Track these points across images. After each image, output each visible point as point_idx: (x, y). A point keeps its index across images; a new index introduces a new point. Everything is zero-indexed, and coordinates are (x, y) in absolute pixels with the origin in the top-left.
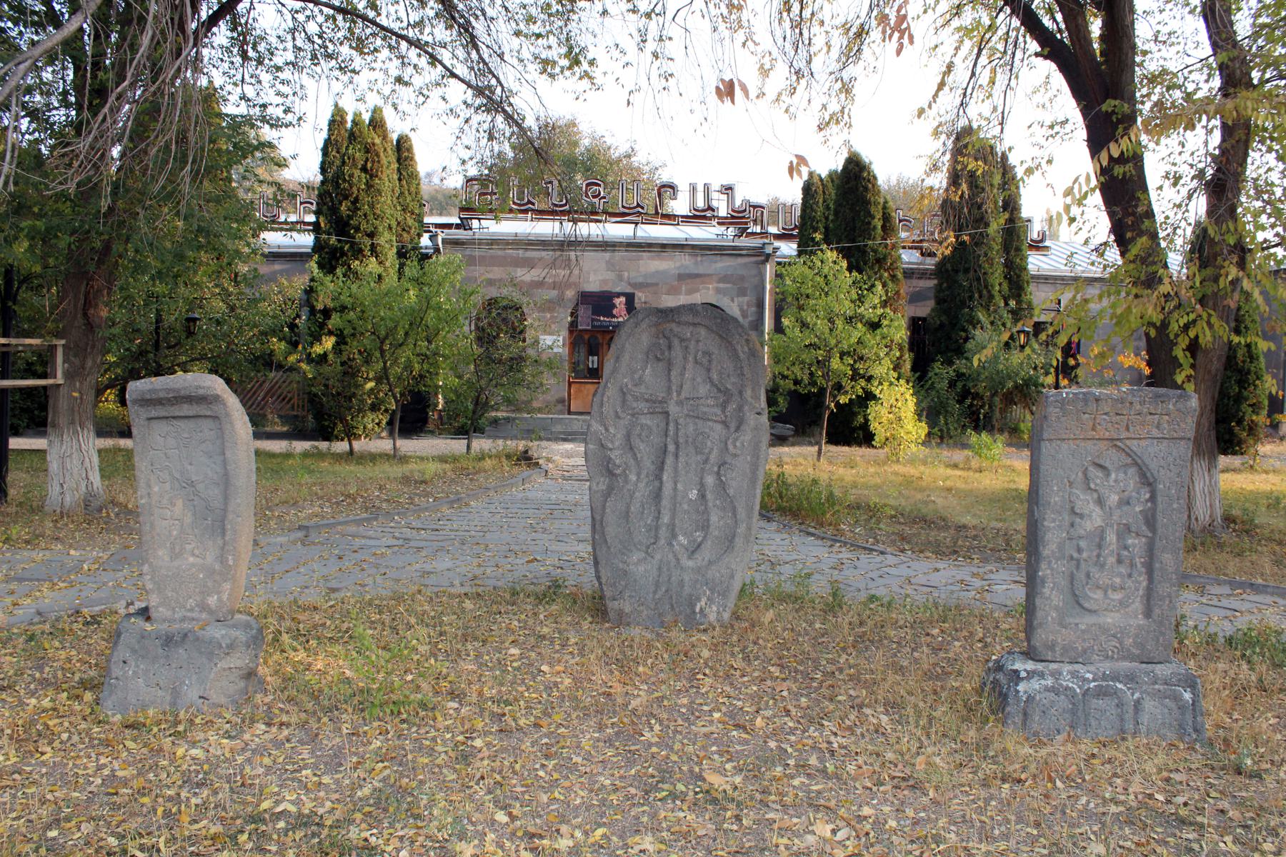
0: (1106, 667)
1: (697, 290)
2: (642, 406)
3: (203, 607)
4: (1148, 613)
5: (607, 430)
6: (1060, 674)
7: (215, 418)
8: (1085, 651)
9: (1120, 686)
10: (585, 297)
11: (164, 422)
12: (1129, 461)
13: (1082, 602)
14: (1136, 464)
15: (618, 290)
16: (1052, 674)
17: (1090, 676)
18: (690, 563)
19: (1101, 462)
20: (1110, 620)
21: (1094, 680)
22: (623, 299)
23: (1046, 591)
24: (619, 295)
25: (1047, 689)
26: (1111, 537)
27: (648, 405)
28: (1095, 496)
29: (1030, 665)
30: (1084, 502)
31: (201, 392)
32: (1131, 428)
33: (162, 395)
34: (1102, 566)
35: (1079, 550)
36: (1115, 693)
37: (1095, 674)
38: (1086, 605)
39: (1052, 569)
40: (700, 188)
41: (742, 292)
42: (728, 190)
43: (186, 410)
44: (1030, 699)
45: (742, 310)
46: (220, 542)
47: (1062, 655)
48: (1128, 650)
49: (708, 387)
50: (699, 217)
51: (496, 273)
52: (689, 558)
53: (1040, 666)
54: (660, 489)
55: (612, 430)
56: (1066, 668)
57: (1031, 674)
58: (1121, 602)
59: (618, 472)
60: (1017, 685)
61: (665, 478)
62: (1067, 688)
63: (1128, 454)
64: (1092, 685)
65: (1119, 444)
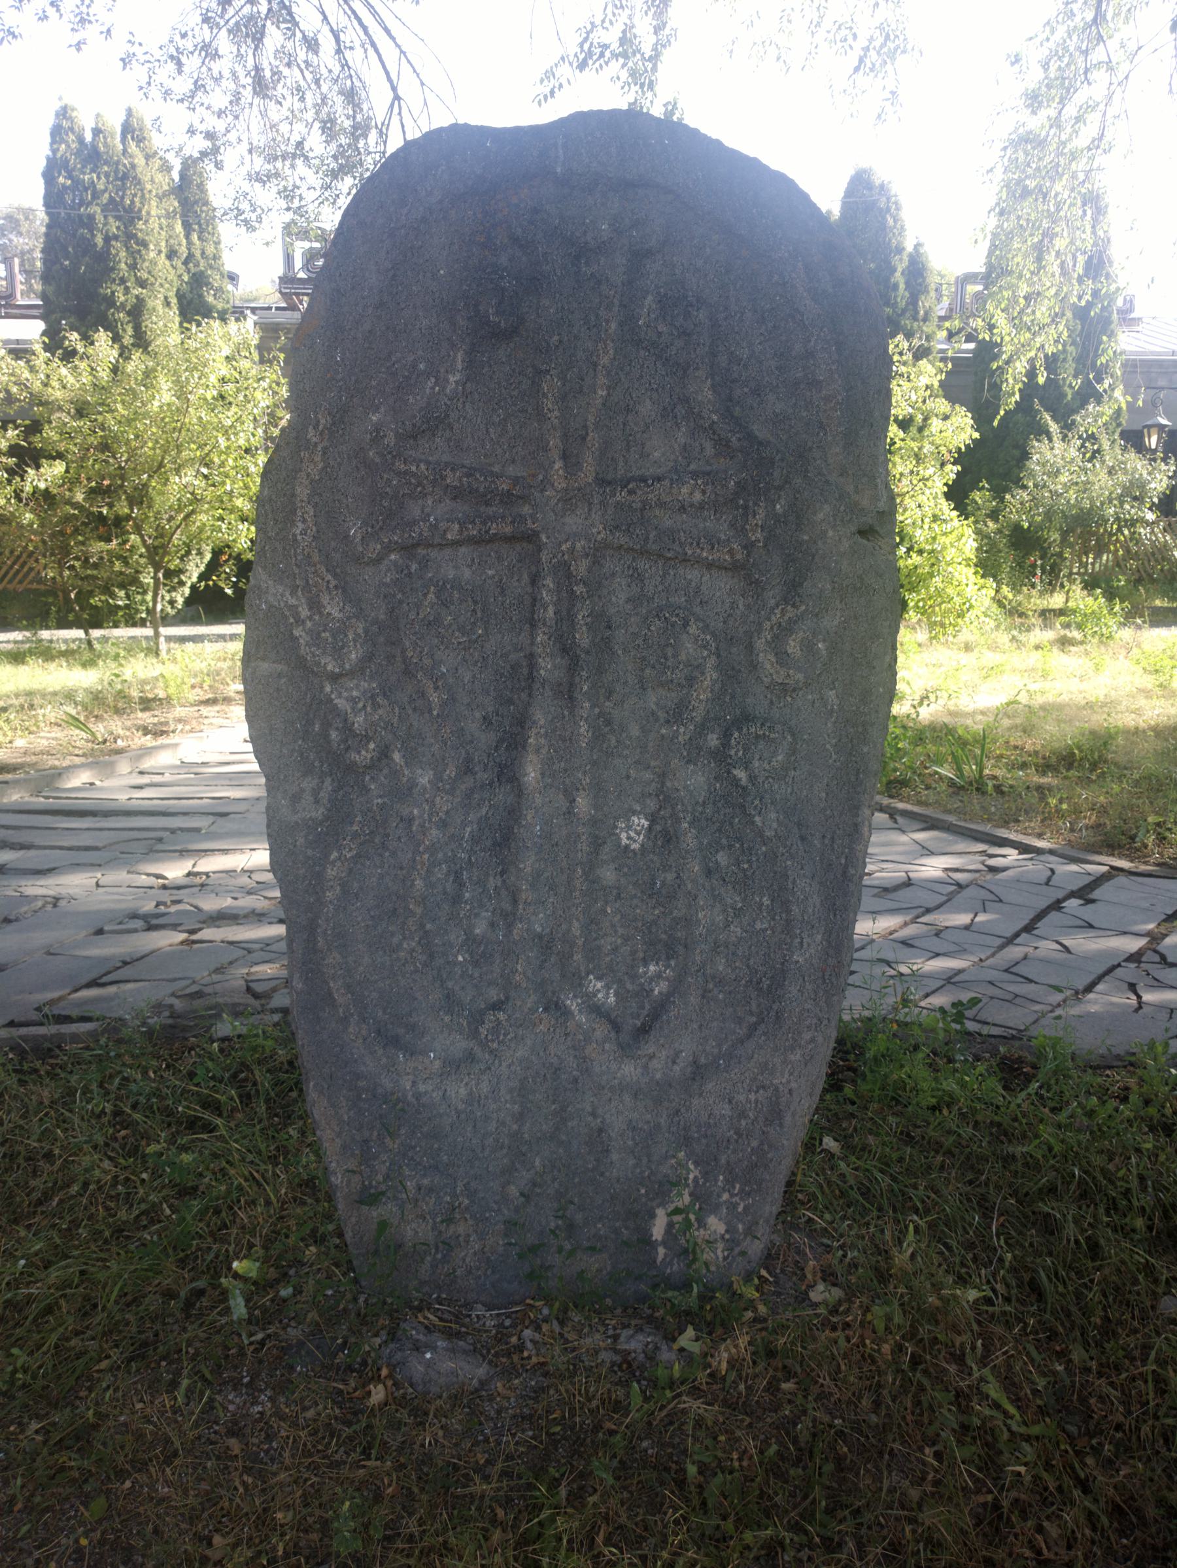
5: (315, 605)
18: (629, 1070)
54: (514, 813)
61: (531, 774)
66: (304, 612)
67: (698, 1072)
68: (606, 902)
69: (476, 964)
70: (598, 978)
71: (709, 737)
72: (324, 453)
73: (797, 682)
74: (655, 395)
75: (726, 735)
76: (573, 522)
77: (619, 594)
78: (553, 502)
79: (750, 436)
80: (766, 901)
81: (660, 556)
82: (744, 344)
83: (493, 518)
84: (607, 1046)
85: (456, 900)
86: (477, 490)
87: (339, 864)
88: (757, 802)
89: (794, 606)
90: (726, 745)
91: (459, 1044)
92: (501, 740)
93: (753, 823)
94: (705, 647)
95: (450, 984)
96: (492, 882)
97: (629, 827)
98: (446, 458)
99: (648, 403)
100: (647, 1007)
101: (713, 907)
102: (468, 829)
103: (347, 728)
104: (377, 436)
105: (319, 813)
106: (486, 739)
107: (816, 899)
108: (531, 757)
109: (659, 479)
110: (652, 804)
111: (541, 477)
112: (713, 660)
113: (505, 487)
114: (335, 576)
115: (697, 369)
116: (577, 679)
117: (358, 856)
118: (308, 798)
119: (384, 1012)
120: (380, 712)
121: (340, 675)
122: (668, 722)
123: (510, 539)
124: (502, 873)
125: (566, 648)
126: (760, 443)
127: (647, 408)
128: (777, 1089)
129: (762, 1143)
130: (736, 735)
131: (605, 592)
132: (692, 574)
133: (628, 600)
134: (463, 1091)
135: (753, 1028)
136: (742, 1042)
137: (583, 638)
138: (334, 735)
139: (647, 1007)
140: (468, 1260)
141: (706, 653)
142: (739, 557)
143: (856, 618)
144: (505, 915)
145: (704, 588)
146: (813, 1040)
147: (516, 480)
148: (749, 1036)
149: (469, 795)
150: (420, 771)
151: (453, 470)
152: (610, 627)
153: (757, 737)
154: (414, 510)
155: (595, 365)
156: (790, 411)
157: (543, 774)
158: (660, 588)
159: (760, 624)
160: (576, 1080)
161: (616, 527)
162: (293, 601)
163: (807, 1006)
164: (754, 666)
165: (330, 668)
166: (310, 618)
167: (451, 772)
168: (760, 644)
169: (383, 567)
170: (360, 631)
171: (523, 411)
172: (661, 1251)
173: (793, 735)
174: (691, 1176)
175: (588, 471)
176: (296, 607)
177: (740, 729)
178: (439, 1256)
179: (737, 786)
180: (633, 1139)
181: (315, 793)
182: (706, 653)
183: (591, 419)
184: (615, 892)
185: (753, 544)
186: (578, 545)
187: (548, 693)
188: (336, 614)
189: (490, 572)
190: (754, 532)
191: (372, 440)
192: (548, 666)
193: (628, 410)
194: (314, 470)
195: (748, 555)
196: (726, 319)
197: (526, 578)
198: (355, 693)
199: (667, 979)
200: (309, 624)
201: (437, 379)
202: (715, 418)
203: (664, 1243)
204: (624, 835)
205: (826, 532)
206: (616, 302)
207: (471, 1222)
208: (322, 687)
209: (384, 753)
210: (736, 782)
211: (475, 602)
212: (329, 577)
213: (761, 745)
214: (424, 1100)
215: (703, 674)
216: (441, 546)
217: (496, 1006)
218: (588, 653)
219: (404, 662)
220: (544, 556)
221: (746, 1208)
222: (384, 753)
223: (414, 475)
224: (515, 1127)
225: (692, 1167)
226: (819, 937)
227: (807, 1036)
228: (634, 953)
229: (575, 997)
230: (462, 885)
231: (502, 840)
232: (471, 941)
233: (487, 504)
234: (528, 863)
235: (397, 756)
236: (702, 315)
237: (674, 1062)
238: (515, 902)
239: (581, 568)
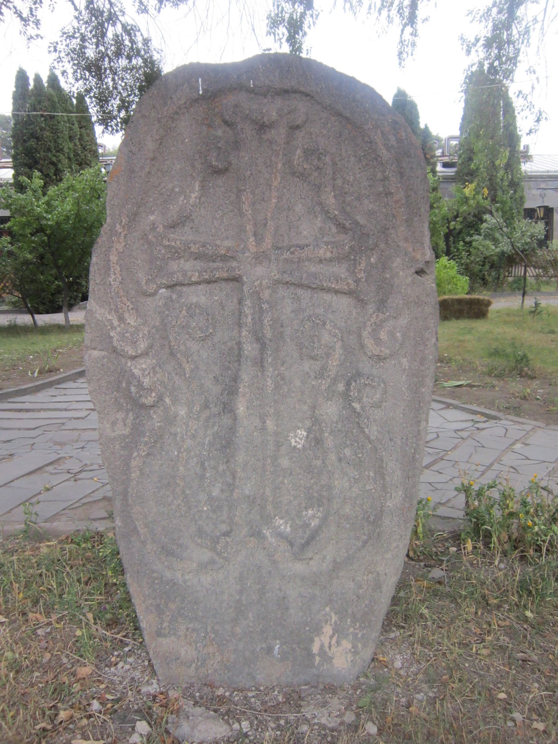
2: (190, 268)
5: (121, 319)
18: (299, 567)
27: (199, 265)
49: (318, 222)
54: (232, 430)
55: (131, 320)
59: (149, 400)
61: (241, 409)
66: (116, 323)
67: (336, 566)
68: (284, 477)
69: (214, 511)
70: (281, 518)
71: (339, 386)
72: (125, 237)
73: (386, 354)
74: (303, 201)
75: (348, 384)
76: (260, 270)
77: (287, 308)
78: (249, 259)
79: (357, 223)
80: (372, 474)
81: (309, 287)
82: (351, 174)
83: (217, 269)
84: (287, 554)
85: (202, 477)
86: (208, 254)
87: (138, 459)
88: (366, 421)
89: (383, 313)
90: (348, 389)
91: (206, 555)
92: (224, 390)
93: (364, 432)
94: (335, 336)
95: (200, 523)
96: (221, 468)
97: (296, 436)
98: (191, 238)
99: (300, 205)
100: (308, 533)
101: (343, 478)
102: (208, 439)
103: (140, 385)
104: (153, 227)
105: (127, 431)
106: (216, 389)
107: (398, 473)
108: (240, 399)
109: (307, 246)
110: (308, 423)
111: (242, 246)
112: (340, 344)
113: (223, 252)
114: (132, 303)
115: (326, 187)
116: (265, 355)
117: (148, 454)
118: (120, 424)
119: (165, 537)
120: (158, 376)
121: (136, 357)
122: (316, 377)
123: (227, 280)
124: (227, 462)
125: (259, 339)
126: (362, 226)
127: (299, 208)
128: (378, 573)
129: (371, 602)
130: (354, 384)
131: (279, 307)
132: (327, 297)
133: (292, 311)
134: (209, 579)
135: (365, 542)
136: (360, 550)
137: (268, 333)
138: (133, 389)
139: (308, 533)
140: (215, 665)
141: (335, 340)
142: (352, 287)
143: (416, 318)
144: (229, 485)
145: (333, 304)
146: (397, 546)
147: (229, 249)
148: (363, 546)
149: (208, 419)
150: (180, 408)
151: (194, 244)
152: (282, 326)
153: (365, 385)
154: (174, 266)
155: (270, 186)
156: (377, 208)
157: (247, 408)
158: (310, 304)
159: (365, 323)
160: (270, 572)
161: (285, 272)
162: (110, 317)
163: (394, 529)
164: (362, 346)
165: (130, 352)
166: (119, 326)
167: (197, 408)
168: (365, 334)
169: (158, 297)
170: (146, 332)
171: (232, 211)
172: (317, 659)
173: (384, 383)
174: (333, 620)
175: (268, 242)
176: (111, 320)
177: (355, 381)
178: (199, 664)
179: (355, 412)
180: (302, 602)
181: (124, 420)
182: (335, 340)
183: (269, 215)
184: (289, 471)
185: (359, 280)
186: (264, 282)
187: (249, 363)
188: (132, 323)
189: (216, 298)
190: (360, 273)
191: (151, 229)
192: (250, 349)
193: (289, 209)
194: (120, 247)
195: (357, 286)
196: (340, 160)
197: (235, 300)
198: (144, 366)
199: (318, 518)
200: (118, 329)
201: (185, 196)
202: (336, 213)
203: (319, 655)
204: (293, 441)
205: (399, 273)
206: (281, 153)
207: (216, 646)
208: (126, 363)
209: (160, 398)
210: (354, 410)
211: (208, 315)
212: (129, 304)
213: (368, 389)
214: (189, 583)
215: (334, 351)
216: (189, 285)
217: (227, 534)
218: (271, 341)
219: (170, 347)
220: (245, 288)
221: (363, 636)
223: (173, 247)
224: (238, 597)
225: (333, 615)
226: (400, 493)
227: (394, 545)
228: (300, 504)
229: (268, 528)
230: (205, 469)
231: (226, 444)
232: (211, 499)
233: (214, 261)
234: (241, 457)
235: (167, 400)
236: (327, 159)
237: (323, 562)
238: (234, 478)
239: (266, 294)
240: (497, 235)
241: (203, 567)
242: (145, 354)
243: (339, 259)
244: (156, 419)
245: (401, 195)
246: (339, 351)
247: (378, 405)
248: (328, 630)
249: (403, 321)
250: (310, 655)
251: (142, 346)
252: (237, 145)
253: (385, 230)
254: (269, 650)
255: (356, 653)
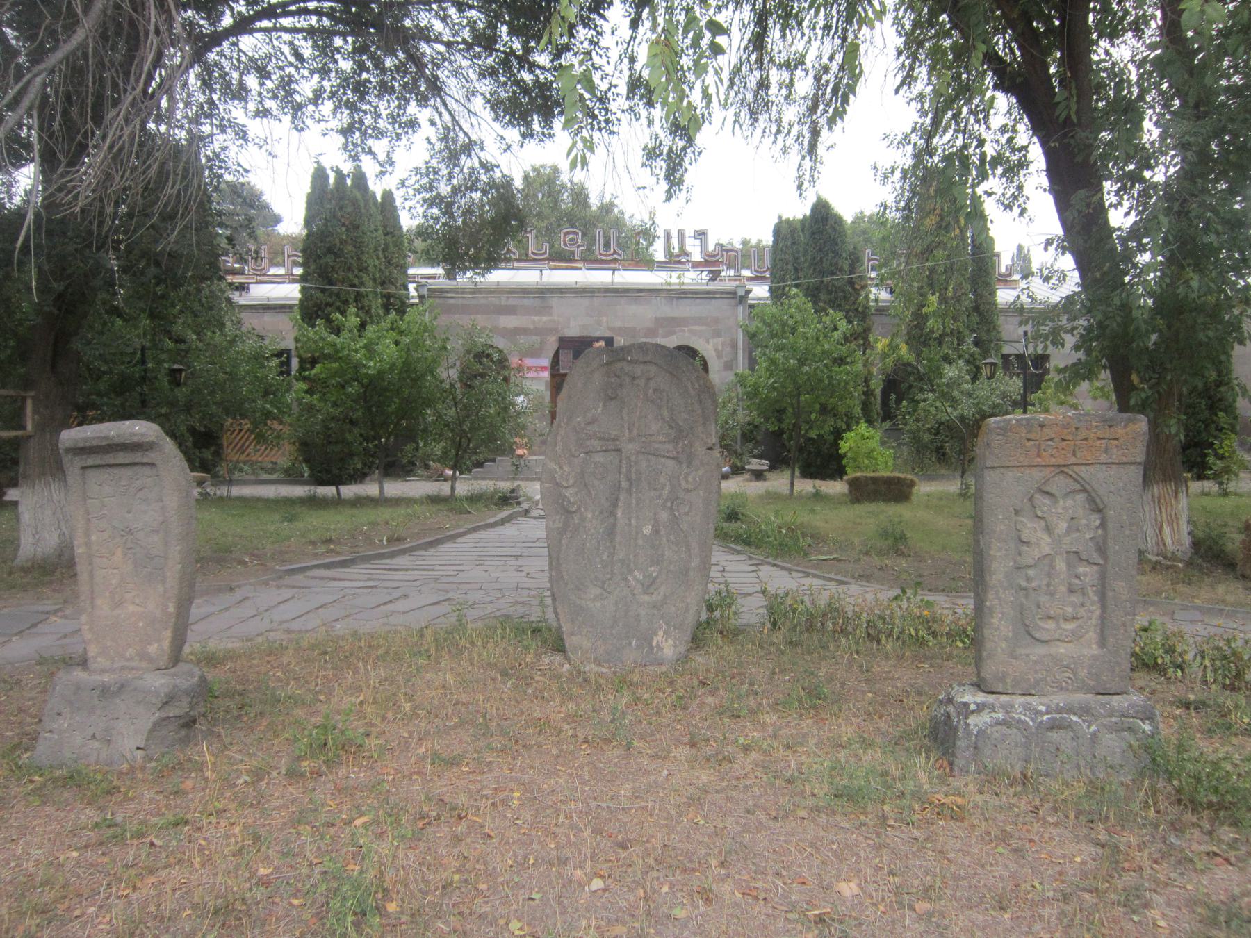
0: (1059, 699)
1: (675, 333)
2: (595, 444)
3: (143, 656)
4: (1102, 643)
5: (561, 468)
6: (1012, 706)
7: (152, 465)
8: (1037, 682)
9: (1074, 718)
10: (564, 343)
11: (103, 470)
12: (1078, 487)
13: (1033, 633)
14: (1085, 490)
15: (597, 334)
16: (1003, 707)
17: (1042, 708)
18: (647, 598)
19: (1047, 489)
20: (1062, 651)
21: (1047, 713)
22: (602, 343)
23: (995, 621)
24: (598, 339)
25: (998, 723)
26: (1061, 565)
28: (1043, 523)
29: (981, 698)
30: (1031, 528)
31: (135, 439)
32: (1078, 455)
33: (95, 443)
34: (1052, 594)
35: (1028, 579)
36: (1069, 726)
37: (1048, 706)
38: (1038, 635)
39: (1000, 599)
40: (675, 235)
41: (717, 334)
42: (701, 235)
43: (122, 458)
44: (981, 732)
45: (716, 350)
46: (160, 589)
47: (1013, 686)
48: (1083, 681)
50: (675, 261)
51: (482, 321)
52: (645, 593)
53: (991, 699)
54: (614, 525)
55: (566, 469)
56: (1018, 700)
57: (981, 708)
58: (1073, 631)
59: (574, 509)
60: (967, 718)
61: (619, 514)
62: (1019, 721)
63: (1075, 480)
64: (1045, 718)
65: (1066, 470)
76: (631, 446)
77: (644, 464)
103: (569, 501)
104: (579, 424)
125: (629, 479)
154: (588, 443)
175: (635, 432)
192: (624, 484)
209: (579, 508)
222: (579, 508)
231: (611, 532)
234: (618, 538)
239: (633, 458)
240: (956, 393)
241: (597, 598)
242: (573, 486)
243: (669, 442)
244: (576, 519)
245: (699, 412)
246: (668, 487)
247: (687, 514)
248: (661, 633)
249: (700, 473)
250: (651, 648)
251: (571, 481)
252: (621, 386)
253: (691, 428)
254: (630, 644)
255: (675, 647)
